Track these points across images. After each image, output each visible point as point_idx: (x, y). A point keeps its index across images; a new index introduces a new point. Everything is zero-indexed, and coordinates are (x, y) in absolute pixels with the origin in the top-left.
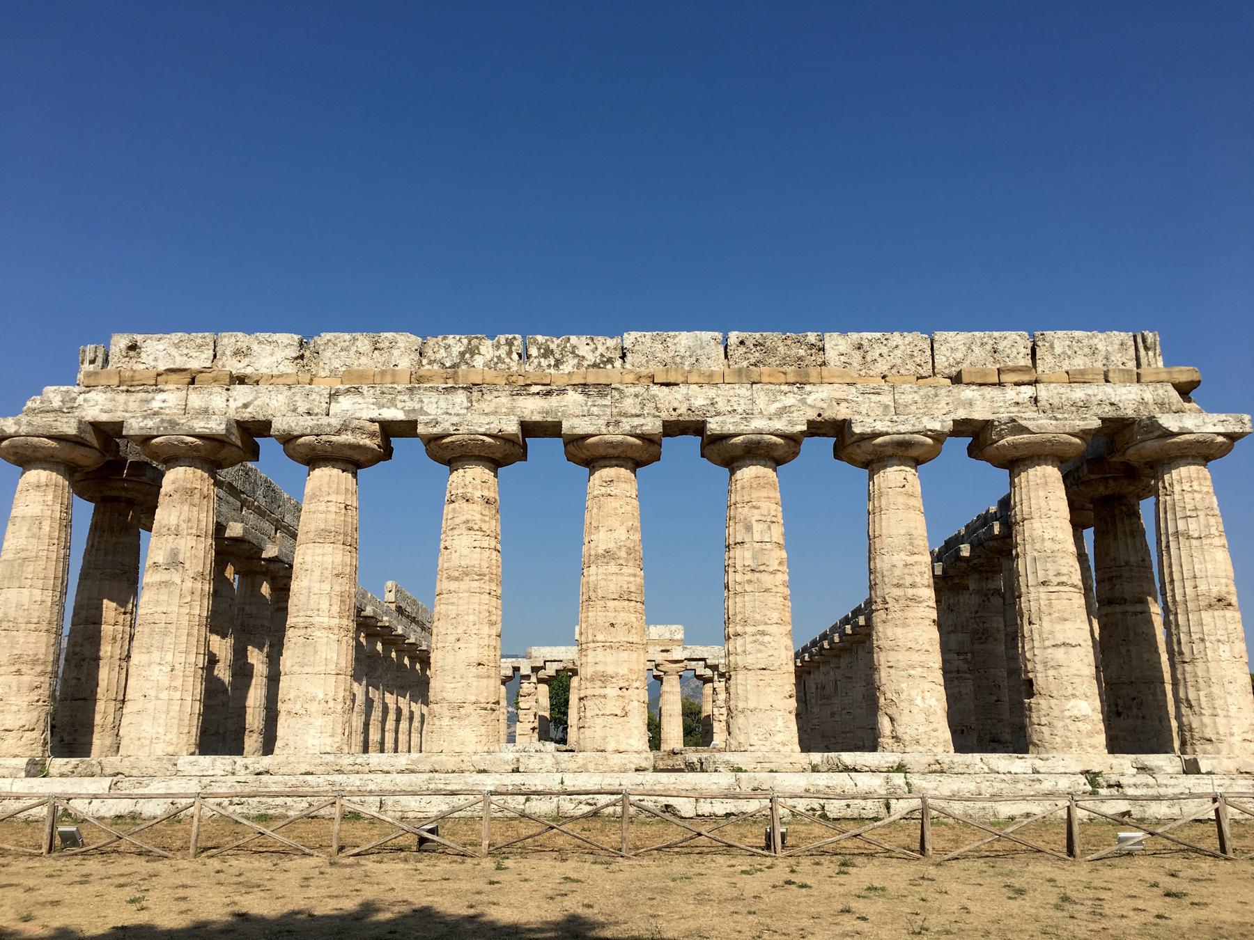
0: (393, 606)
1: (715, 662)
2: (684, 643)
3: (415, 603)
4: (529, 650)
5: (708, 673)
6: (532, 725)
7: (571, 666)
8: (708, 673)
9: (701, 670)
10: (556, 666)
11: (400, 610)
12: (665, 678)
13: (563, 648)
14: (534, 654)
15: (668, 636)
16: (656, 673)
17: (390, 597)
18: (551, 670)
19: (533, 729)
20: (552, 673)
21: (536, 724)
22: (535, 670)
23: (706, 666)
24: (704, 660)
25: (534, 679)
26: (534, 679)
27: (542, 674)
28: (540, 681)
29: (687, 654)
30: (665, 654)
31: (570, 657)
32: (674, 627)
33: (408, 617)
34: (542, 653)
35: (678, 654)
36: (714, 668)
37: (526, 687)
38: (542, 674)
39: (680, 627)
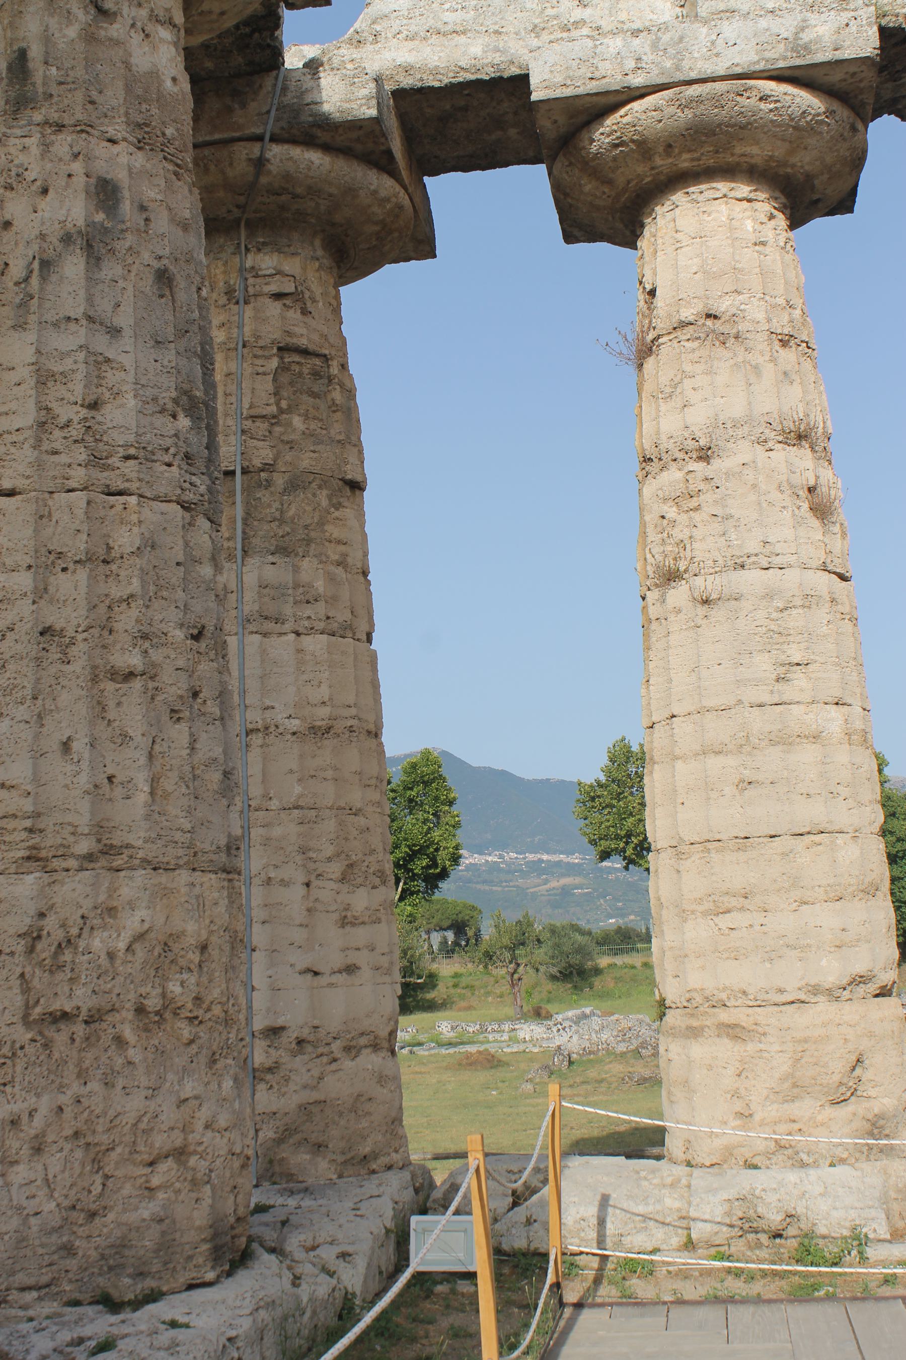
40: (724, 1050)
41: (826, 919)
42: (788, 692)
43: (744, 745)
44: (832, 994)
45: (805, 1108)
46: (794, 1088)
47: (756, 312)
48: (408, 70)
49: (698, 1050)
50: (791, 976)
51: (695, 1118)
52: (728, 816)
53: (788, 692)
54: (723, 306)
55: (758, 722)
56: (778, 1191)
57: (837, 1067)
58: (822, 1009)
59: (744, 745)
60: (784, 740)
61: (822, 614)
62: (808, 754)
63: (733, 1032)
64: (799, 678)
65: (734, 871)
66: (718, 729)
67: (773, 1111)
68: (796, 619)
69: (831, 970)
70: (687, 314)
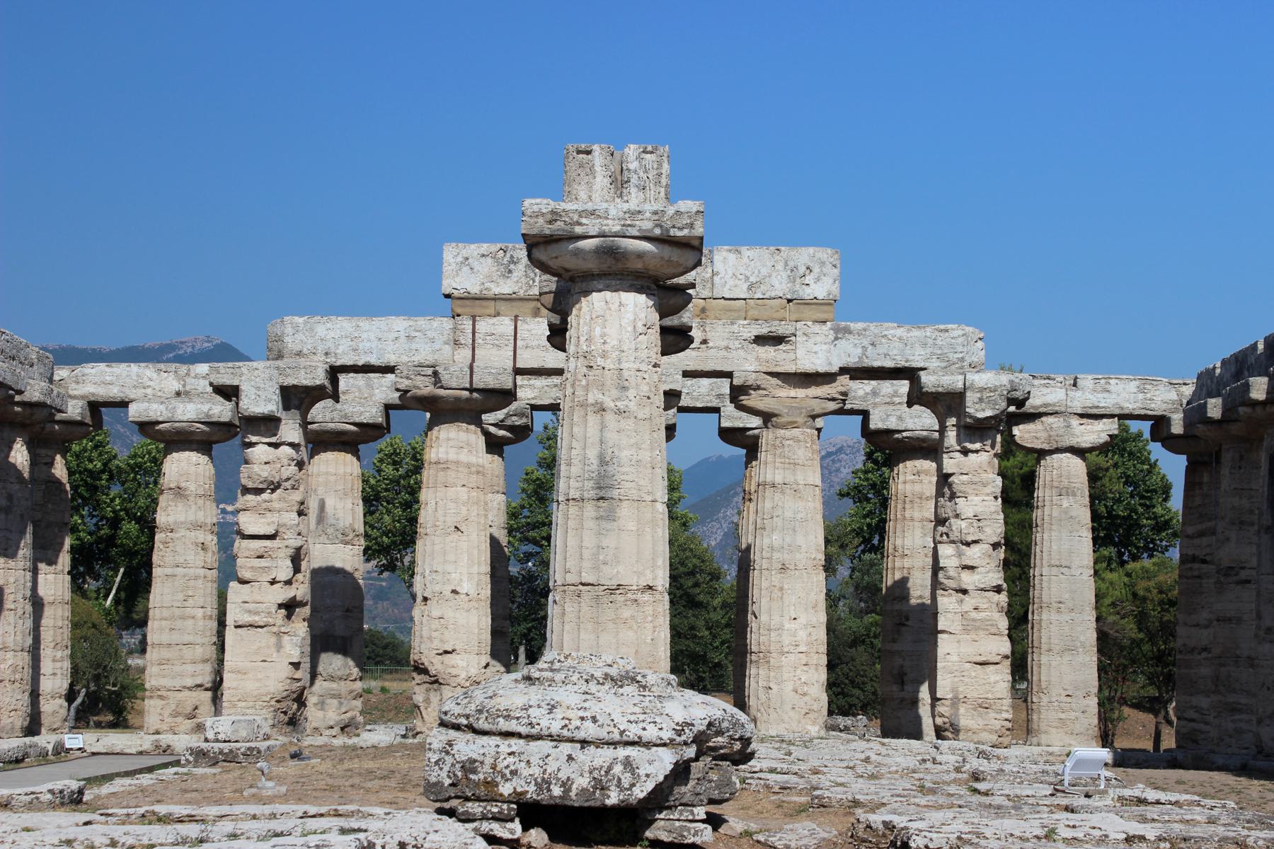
1: (953, 381)
5: (921, 421)
6: (283, 594)
7: (425, 387)
8: (921, 421)
9: (891, 409)
10: (383, 389)
12: (767, 437)
13: (400, 324)
14: (292, 342)
15: (780, 285)
16: (732, 417)
18: (362, 401)
19: (290, 607)
20: (371, 413)
21: (301, 590)
23: (918, 397)
24: (909, 373)
25: (290, 430)
26: (290, 430)
28: (320, 441)
29: (848, 353)
30: (768, 352)
31: (425, 354)
32: (803, 256)
34: (319, 339)
35: (815, 350)
36: (947, 403)
37: (263, 458)
38: (322, 413)
39: (825, 254)
40: (160, 703)
41: (190, 668)
42: (187, 604)
43: (172, 618)
44: (190, 689)
45: (179, 719)
46: (175, 714)
47: (192, 487)
48: (93, 395)
49: (152, 702)
50: (178, 683)
52: (165, 638)
53: (187, 604)
54: (183, 485)
55: (177, 612)
56: (165, 739)
57: (189, 709)
58: (187, 693)
59: (172, 618)
60: (183, 618)
61: (200, 581)
62: (190, 622)
63: (161, 697)
64: (190, 600)
65: (165, 653)
66: (166, 613)
67: (170, 720)
68: (192, 583)
69: (190, 682)
70: (172, 486)
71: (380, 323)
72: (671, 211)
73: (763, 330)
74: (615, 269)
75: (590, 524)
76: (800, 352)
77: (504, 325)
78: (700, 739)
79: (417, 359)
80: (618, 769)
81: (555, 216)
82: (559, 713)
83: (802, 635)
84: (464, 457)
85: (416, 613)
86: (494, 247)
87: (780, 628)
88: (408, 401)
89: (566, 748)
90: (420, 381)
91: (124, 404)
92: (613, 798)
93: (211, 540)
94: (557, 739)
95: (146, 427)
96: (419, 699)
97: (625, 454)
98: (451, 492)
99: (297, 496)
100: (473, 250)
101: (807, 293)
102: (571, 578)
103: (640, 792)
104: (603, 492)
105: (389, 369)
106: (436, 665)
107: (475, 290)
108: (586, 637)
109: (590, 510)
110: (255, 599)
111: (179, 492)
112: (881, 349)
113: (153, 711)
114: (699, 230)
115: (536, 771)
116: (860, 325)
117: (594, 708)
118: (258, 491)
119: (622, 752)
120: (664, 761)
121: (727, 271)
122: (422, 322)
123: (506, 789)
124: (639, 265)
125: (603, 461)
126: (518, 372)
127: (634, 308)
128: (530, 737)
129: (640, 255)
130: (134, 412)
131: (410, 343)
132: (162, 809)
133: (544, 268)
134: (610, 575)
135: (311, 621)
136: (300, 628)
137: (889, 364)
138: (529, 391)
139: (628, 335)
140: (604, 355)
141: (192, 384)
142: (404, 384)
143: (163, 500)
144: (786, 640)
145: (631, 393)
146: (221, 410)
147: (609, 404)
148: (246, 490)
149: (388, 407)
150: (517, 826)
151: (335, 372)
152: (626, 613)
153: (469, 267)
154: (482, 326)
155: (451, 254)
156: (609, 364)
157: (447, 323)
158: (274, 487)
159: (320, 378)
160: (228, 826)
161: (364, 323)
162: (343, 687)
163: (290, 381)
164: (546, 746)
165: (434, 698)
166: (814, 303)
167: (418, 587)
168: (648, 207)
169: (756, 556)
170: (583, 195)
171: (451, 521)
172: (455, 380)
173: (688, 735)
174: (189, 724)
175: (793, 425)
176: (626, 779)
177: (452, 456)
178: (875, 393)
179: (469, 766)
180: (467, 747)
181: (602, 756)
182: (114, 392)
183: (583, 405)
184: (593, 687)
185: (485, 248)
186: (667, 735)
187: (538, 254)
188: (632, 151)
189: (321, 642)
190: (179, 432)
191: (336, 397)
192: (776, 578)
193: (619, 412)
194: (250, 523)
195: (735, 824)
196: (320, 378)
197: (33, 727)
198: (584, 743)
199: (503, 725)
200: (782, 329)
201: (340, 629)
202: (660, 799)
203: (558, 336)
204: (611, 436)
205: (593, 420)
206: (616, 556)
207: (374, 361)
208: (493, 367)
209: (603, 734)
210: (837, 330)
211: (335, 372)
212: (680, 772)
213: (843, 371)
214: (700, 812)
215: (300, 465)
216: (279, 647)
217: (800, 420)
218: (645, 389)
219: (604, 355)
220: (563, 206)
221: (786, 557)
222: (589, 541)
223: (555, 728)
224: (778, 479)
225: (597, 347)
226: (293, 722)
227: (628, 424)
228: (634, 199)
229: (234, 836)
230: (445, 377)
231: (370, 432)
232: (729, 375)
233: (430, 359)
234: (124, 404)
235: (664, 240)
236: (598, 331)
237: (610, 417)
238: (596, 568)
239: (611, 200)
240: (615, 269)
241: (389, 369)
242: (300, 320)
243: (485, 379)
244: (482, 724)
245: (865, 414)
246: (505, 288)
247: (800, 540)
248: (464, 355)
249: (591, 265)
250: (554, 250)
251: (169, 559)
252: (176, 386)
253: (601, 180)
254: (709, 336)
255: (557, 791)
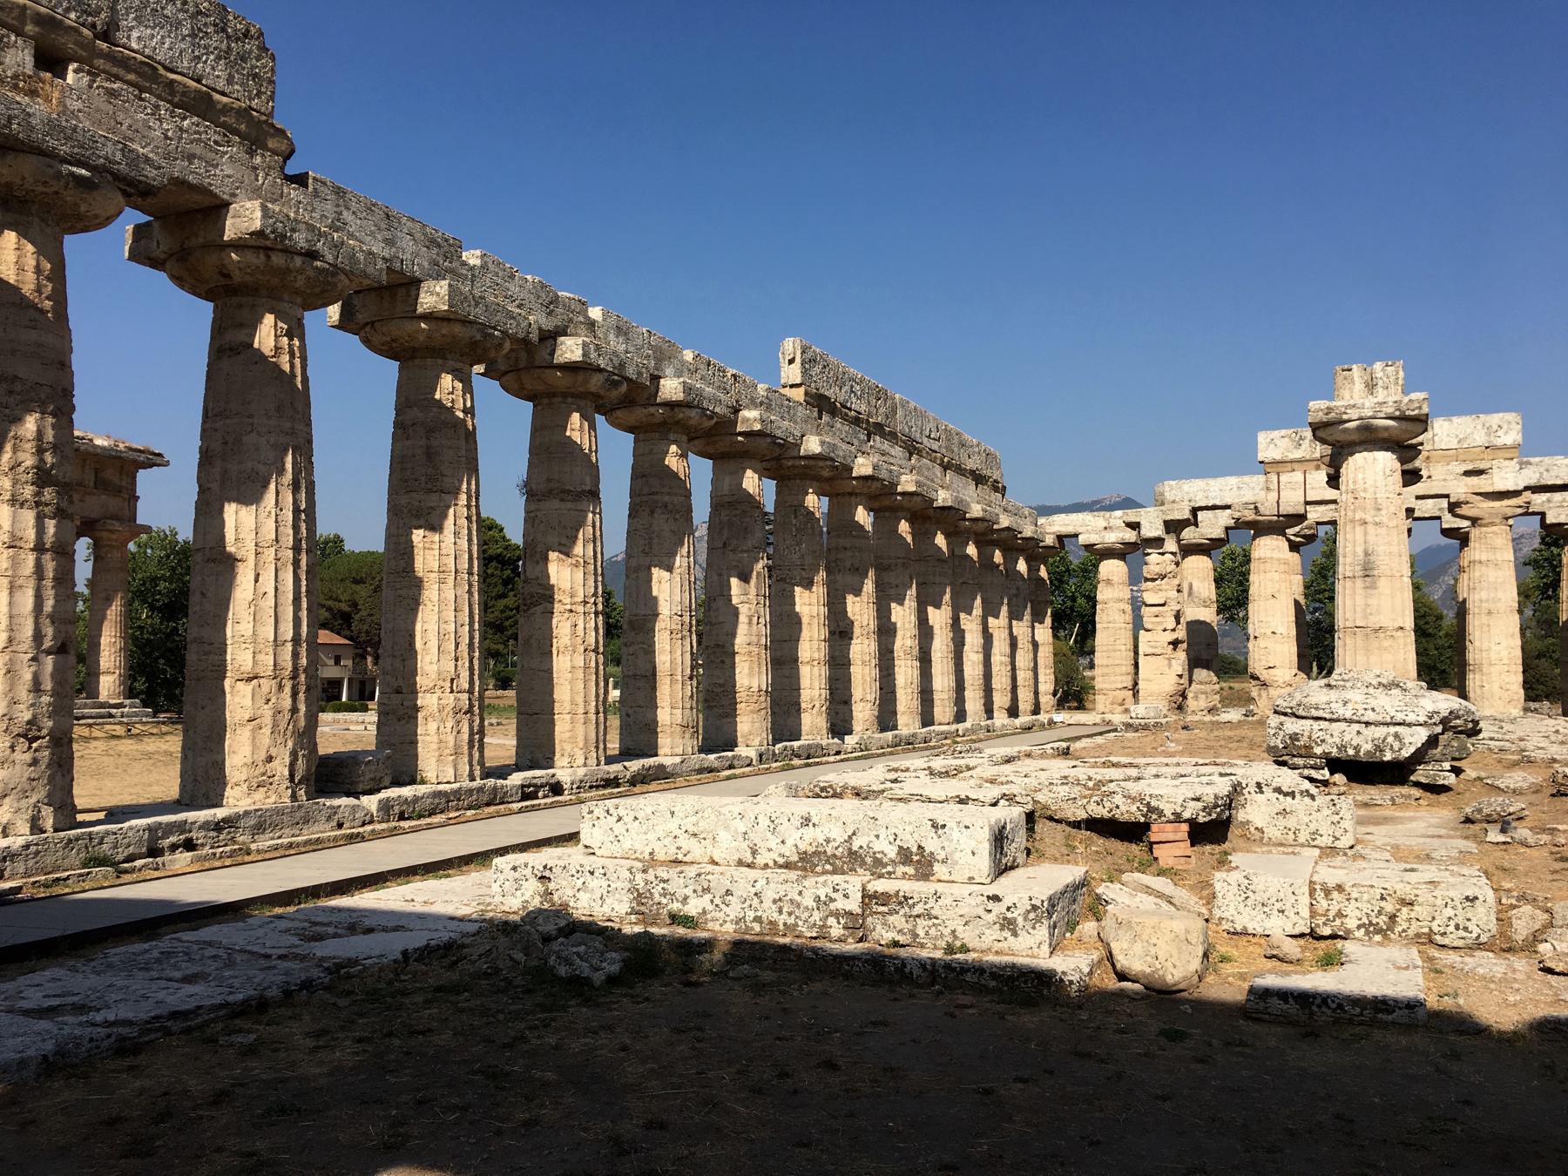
0: (798, 395)
2: (1522, 452)
3: (880, 394)
4: (1159, 489)
6: (1171, 637)
7: (1250, 516)
10: (1225, 518)
11: (820, 403)
12: (1475, 533)
13: (1233, 481)
14: (1169, 496)
15: (1480, 438)
16: (1449, 522)
17: (793, 373)
18: (1212, 526)
19: (1175, 644)
20: (1218, 533)
21: (1181, 634)
22: (1174, 527)
25: (1171, 545)
26: (1171, 545)
27: (1189, 534)
28: (1188, 550)
29: (1530, 476)
30: (1474, 480)
31: (1249, 497)
32: (1495, 419)
33: (856, 421)
34: (1183, 493)
35: (1506, 476)
37: (1155, 561)
38: (1189, 534)
39: (1512, 417)
47: (1115, 579)
51: (1100, 706)
56: (1108, 717)
65: (1106, 670)
71: (1220, 481)
72: (1406, 400)
73: (1470, 467)
74: (1370, 438)
75: (1360, 591)
76: (1496, 479)
77: (1298, 476)
78: (1444, 722)
79: (1245, 500)
80: (1390, 739)
81: (1329, 410)
82: (1350, 706)
83: (1504, 653)
84: (1276, 555)
85: (1250, 645)
86: (1290, 431)
87: (1489, 650)
88: (1240, 525)
89: (1356, 727)
90: (1246, 513)
91: (1076, 536)
92: (1388, 757)
93: (1128, 608)
94: (1351, 721)
95: (1089, 547)
96: (1254, 694)
97: (1381, 549)
98: (1269, 575)
99: (1176, 582)
100: (1276, 434)
101: (1499, 442)
102: (1348, 624)
103: (1406, 753)
104: (1368, 571)
105: (1228, 507)
106: (1264, 675)
107: (1278, 458)
108: (1361, 658)
109: (1359, 583)
110: (1156, 638)
111: (1109, 582)
112: (1553, 473)
113: (1101, 702)
114: (1425, 410)
115: (1338, 741)
116: (1537, 459)
117: (1373, 703)
118: (1153, 580)
119: (1392, 729)
120: (1420, 736)
121: (1444, 433)
122: (1246, 478)
123: (1318, 750)
124: (1386, 435)
125: (1367, 554)
126: (1307, 503)
127: (1386, 461)
128: (1331, 720)
129: (1386, 428)
130: (1082, 539)
131: (1240, 491)
132: (1114, 759)
133: (1323, 441)
134: (1374, 621)
135: (1187, 651)
136: (1181, 656)
137: (1559, 482)
138: (1315, 514)
139: (1380, 477)
140: (1365, 490)
141: (1113, 522)
142: (1237, 515)
143: (1100, 587)
144: (1493, 656)
145: (1384, 512)
146: (1130, 536)
147: (1369, 519)
148: (1147, 580)
149: (1227, 529)
150: (1326, 772)
151: (1195, 511)
152: (1386, 644)
153: (1273, 444)
154: (1284, 478)
155: (1262, 438)
156: (1368, 496)
157: (1262, 478)
158: (1163, 577)
159: (1186, 515)
160: (1154, 771)
161: (1211, 482)
162: (1208, 688)
163: (1169, 518)
164: (1343, 725)
165: (1264, 694)
166: (1505, 448)
167: (1250, 631)
168: (1391, 399)
169: (1470, 605)
170: (1347, 396)
171: (1269, 592)
172: (1268, 510)
173: (1436, 719)
174: (1121, 708)
175: (1493, 524)
176: (1396, 746)
177: (1268, 554)
178: (1549, 501)
179: (1294, 737)
180: (1292, 726)
181: (1380, 732)
182: (1070, 530)
183: (1352, 521)
184: (1371, 690)
185: (1283, 432)
186: (1422, 719)
187: (1319, 433)
188: (1378, 366)
189: (1194, 663)
190: (1107, 549)
191: (1196, 525)
192: (1485, 619)
193: (1376, 524)
194: (1149, 598)
195: (1470, 773)
196: (1186, 515)
197: (1036, 711)
198: (1367, 724)
199: (1314, 713)
200: (1482, 466)
201: (1205, 656)
202: (1419, 757)
203: (1334, 481)
204: (1371, 539)
205: (1359, 530)
206: (1376, 610)
207: (1218, 503)
208: (1292, 501)
209: (1379, 718)
210: (1521, 463)
211: (1195, 511)
212: (1432, 741)
213: (1527, 488)
214: (1447, 766)
215: (1177, 564)
216: (1170, 666)
217: (1497, 521)
218: (1392, 509)
219: (1365, 490)
220: (1333, 404)
221: (1492, 606)
222: (1360, 601)
223: (1348, 715)
224: (1484, 558)
225: (1360, 486)
226: (1180, 708)
227: (1383, 531)
228: (1381, 395)
229: (1157, 776)
230: (1262, 509)
231: (1217, 543)
232: (1447, 496)
233: (1252, 499)
234: (1076, 536)
235: (1402, 418)
236: (1360, 476)
237: (1370, 528)
238: (1365, 617)
239: (1367, 394)
240: (1370, 438)
241: (1228, 507)
242: (1173, 483)
243: (1287, 509)
244: (1301, 712)
245: (1543, 515)
246: (1297, 455)
247: (1500, 594)
248: (1273, 496)
249: (1355, 437)
250: (1330, 430)
251: (1105, 618)
252: (1105, 524)
253: (1359, 386)
254: (1432, 473)
255: (1351, 752)
